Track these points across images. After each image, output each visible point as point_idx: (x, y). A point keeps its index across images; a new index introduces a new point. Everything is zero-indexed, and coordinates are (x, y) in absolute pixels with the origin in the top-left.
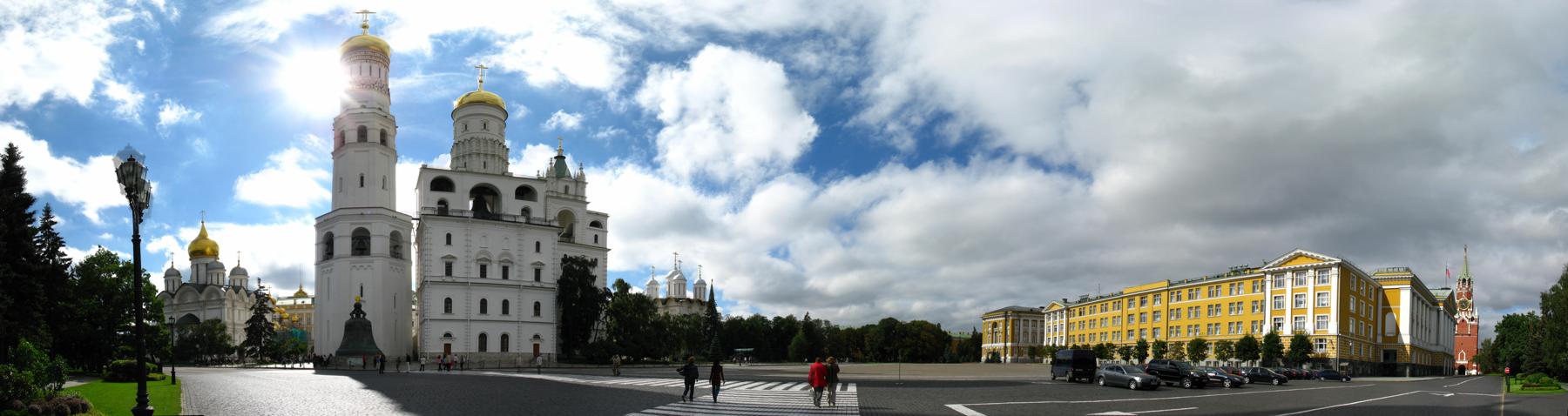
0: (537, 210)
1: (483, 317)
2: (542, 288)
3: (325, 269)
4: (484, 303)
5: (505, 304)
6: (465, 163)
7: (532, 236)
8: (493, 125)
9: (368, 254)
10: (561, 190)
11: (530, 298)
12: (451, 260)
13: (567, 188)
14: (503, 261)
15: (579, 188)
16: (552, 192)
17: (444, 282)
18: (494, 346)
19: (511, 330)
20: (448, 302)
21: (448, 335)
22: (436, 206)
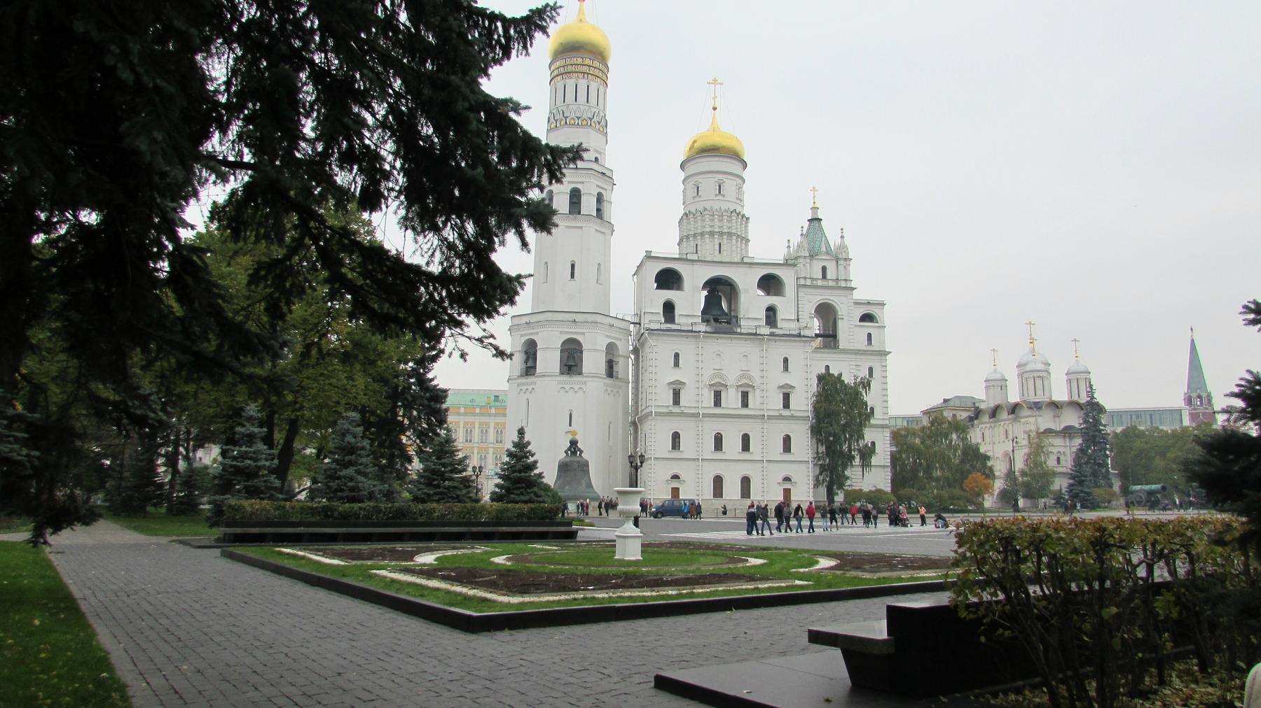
0: (785, 305)
1: (718, 455)
2: (793, 417)
3: (524, 388)
4: (718, 441)
5: (746, 440)
7: (778, 351)
8: (730, 186)
9: (580, 373)
11: (776, 433)
12: (679, 386)
13: (824, 269)
14: (741, 386)
15: (841, 268)
16: (805, 278)
17: (670, 414)
19: (754, 473)
20: (676, 437)
21: (676, 477)
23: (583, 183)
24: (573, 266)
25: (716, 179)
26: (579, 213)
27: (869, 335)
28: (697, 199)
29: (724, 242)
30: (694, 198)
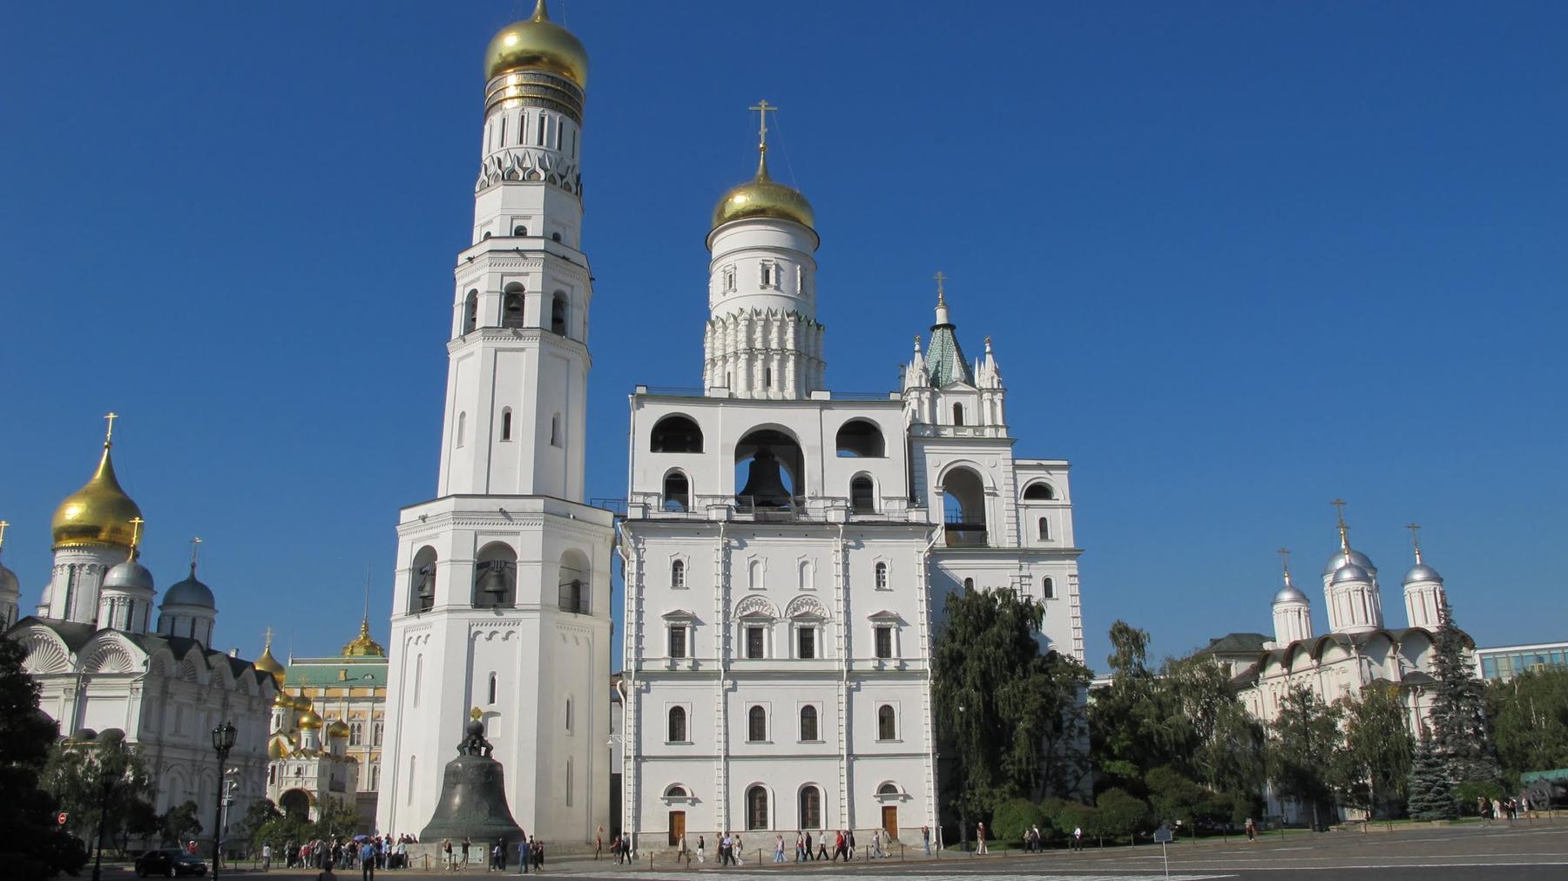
0: (887, 474)
3: (415, 635)
4: (757, 720)
6: (729, 374)
9: (511, 605)
10: (945, 416)
11: (870, 698)
13: (958, 409)
18: (784, 814)
20: (677, 715)
21: (675, 792)
22: (659, 488)
23: (527, 274)
24: (507, 417)
25: (760, 260)
26: (520, 325)
27: (1043, 522)
28: (730, 295)
29: (774, 366)
30: (724, 294)
